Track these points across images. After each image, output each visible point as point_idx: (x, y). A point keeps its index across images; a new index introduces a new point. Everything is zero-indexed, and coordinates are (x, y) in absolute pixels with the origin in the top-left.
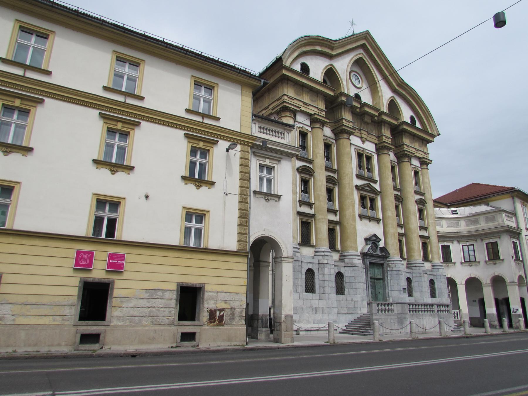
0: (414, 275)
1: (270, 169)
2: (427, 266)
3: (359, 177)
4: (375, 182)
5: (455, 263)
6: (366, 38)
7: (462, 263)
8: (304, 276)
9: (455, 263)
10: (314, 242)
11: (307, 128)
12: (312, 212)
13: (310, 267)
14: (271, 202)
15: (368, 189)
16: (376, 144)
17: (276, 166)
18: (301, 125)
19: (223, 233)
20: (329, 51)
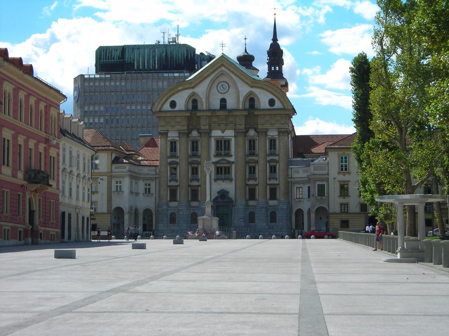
1: (120, 182)
2: (272, 203)
3: (217, 155)
4: (232, 156)
5: (304, 199)
6: (222, 60)
8: (169, 216)
11: (175, 138)
12: (178, 184)
15: (224, 162)
16: (235, 130)
18: (171, 138)
19: (103, 208)
20: (189, 86)
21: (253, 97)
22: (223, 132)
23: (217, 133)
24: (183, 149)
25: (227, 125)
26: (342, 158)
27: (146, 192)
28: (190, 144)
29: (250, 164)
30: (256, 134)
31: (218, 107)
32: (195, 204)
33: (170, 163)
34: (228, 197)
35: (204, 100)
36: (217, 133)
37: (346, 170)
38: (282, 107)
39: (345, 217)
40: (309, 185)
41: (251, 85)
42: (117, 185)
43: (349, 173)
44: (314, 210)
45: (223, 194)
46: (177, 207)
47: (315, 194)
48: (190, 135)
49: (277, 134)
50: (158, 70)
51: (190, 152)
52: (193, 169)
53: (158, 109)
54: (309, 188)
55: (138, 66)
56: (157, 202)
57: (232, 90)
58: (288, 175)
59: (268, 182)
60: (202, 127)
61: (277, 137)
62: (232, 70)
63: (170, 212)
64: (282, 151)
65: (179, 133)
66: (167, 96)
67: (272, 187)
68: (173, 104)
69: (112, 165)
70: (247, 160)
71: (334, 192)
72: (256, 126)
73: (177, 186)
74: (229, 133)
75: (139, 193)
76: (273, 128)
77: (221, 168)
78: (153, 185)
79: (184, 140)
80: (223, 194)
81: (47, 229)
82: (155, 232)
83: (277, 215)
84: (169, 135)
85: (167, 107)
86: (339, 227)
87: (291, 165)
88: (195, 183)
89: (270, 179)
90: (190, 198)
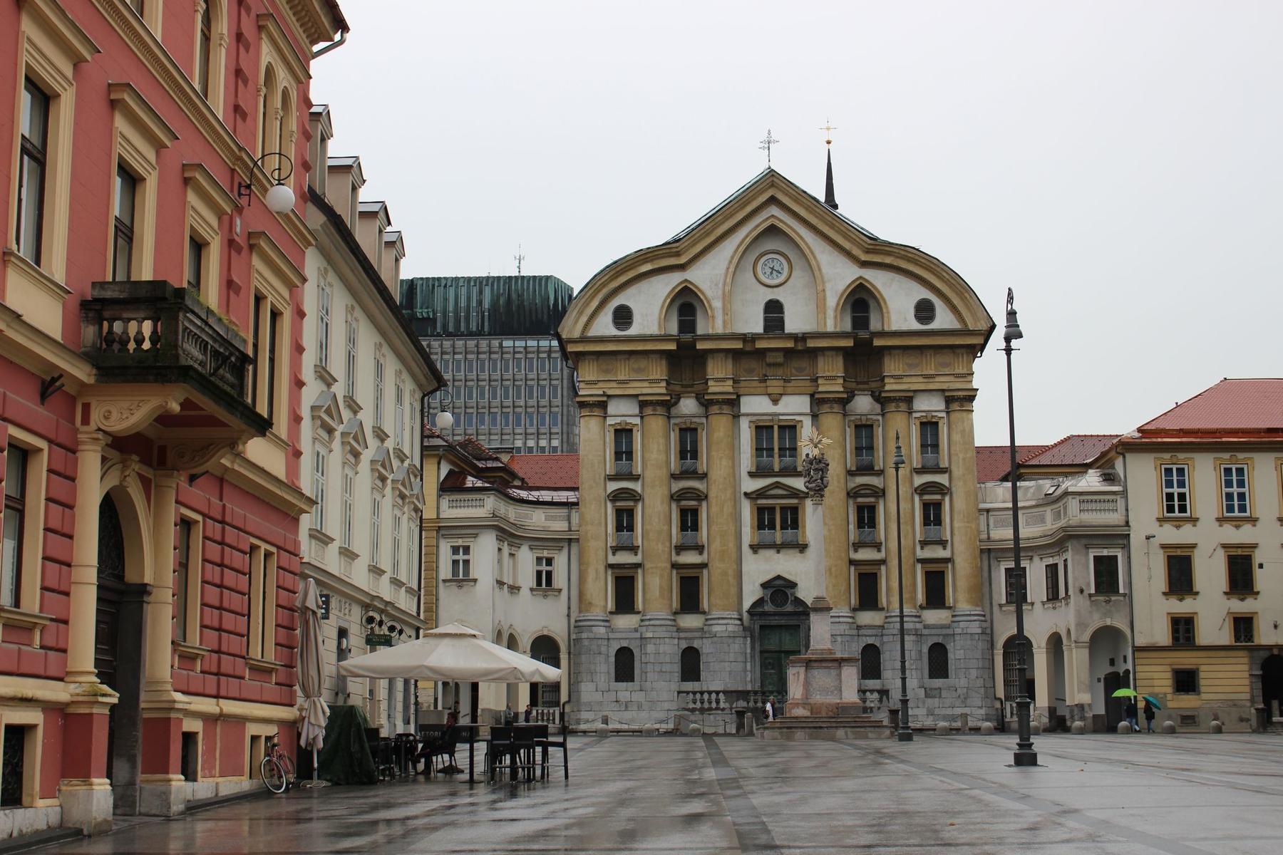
0: (885, 639)
1: (467, 550)
2: (934, 617)
5: (1032, 604)
6: (773, 185)
7: (1043, 603)
8: (613, 659)
9: (1032, 604)
10: (639, 604)
11: (629, 420)
13: (625, 644)
14: (464, 589)
16: (812, 396)
17: (471, 545)
18: (618, 420)
21: (865, 296)
22: (775, 402)
24: (655, 451)
26: (1169, 471)
27: (539, 583)
28: (674, 437)
29: (860, 500)
30: (878, 407)
31: (758, 328)
32: (691, 621)
33: (615, 497)
34: (796, 598)
36: (755, 405)
37: (1183, 509)
38: (956, 325)
39: (1185, 659)
40: (1051, 561)
41: (864, 257)
42: (456, 557)
43: (1194, 521)
44: (1086, 637)
45: (779, 589)
46: (636, 630)
47: (1089, 584)
48: (674, 411)
49: (942, 406)
50: (490, 334)
51: (675, 465)
52: (684, 512)
53: (576, 334)
54: (1052, 570)
55: (445, 326)
56: (574, 616)
57: (799, 278)
58: (979, 532)
60: (714, 387)
61: (944, 415)
62: (803, 213)
63: (616, 646)
64: (961, 456)
65: (643, 405)
66: (605, 291)
67: (933, 567)
68: (623, 316)
69: (439, 496)
70: (851, 485)
71: (1150, 578)
72: (874, 385)
74: (795, 405)
75: (518, 588)
77: (771, 509)
78: (560, 561)
79: (656, 424)
80: (779, 589)
81: (231, 707)
82: (567, 709)
83: (951, 656)
84: (612, 408)
85: (604, 326)
86: (1170, 690)
87: (985, 502)
88: (690, 558)
89: (924, 544)
90: (676, 604)
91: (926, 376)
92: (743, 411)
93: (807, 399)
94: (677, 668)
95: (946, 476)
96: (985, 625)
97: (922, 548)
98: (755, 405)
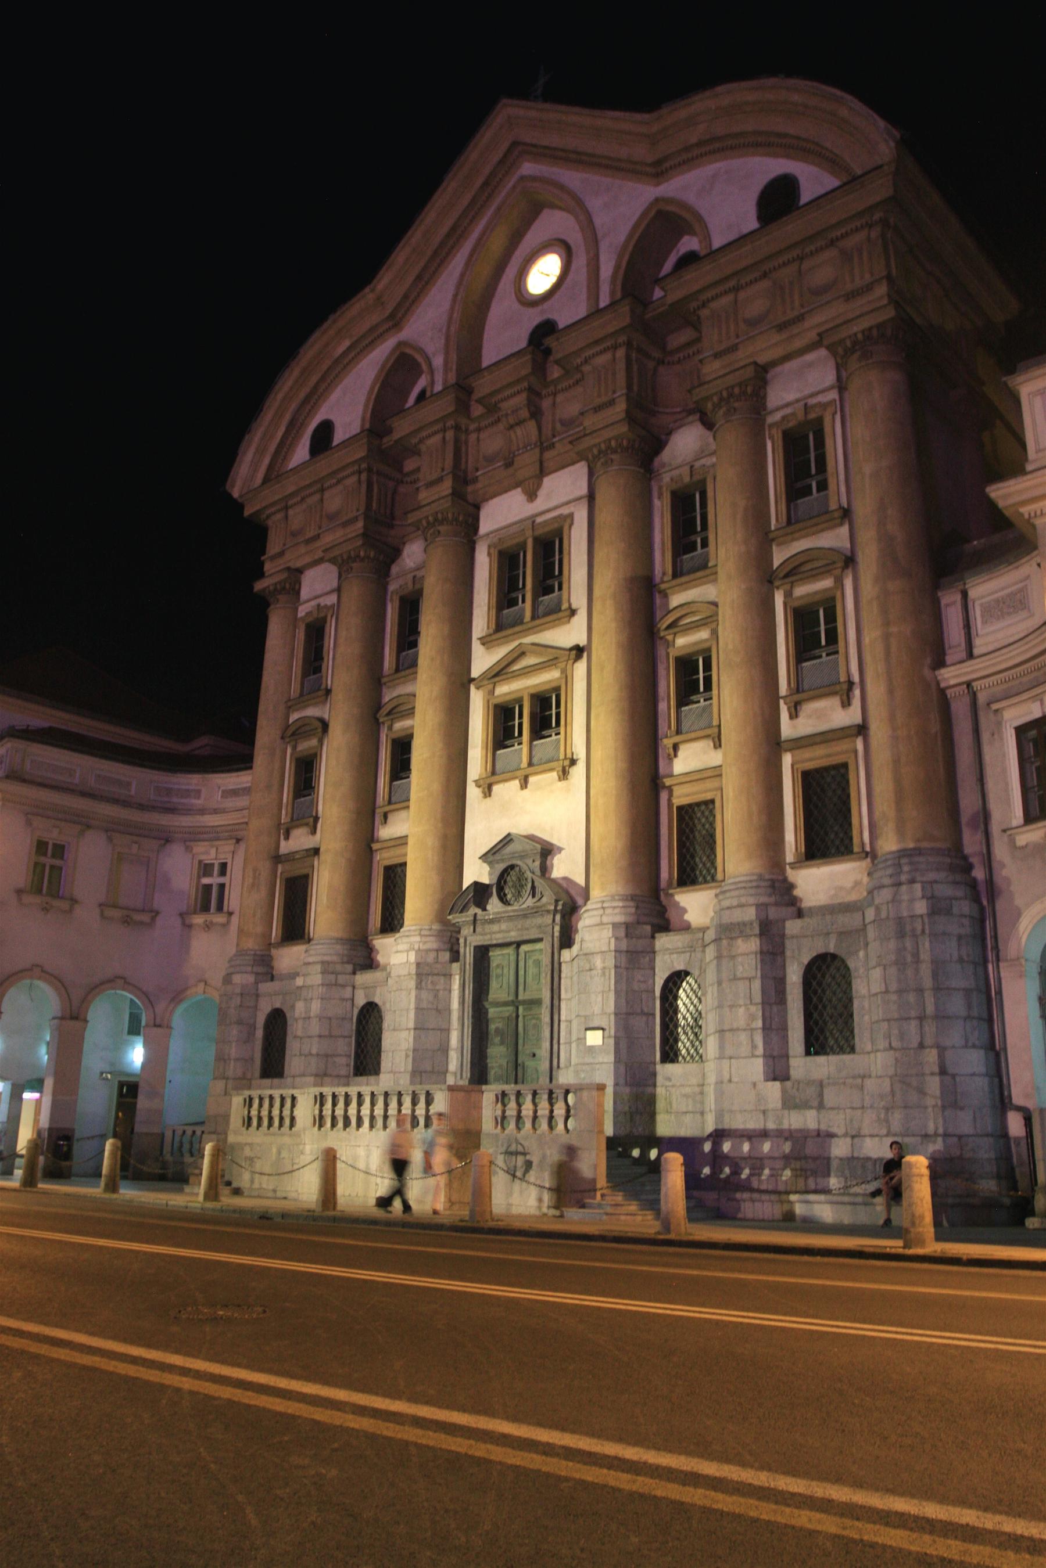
8: (260, 1033)
13: (278, 1005)
23: (503, 513)
25: (544, 446)
35: (438, 361)
48: (395, 569)
59: (788, 728)
61: (833, 395)
63: (265, 1008)
64: (868, 469)
67: (817, 758)
73: (316, 851)
74: (564, 488)
76: (798, 344)
91: (781, 327)
92: (483, 529)
93: (581, 470)
94: (346, 1047)
95: (845, 530)
96: (945, 890)
97: (794, 715)
98: (503, 513)
